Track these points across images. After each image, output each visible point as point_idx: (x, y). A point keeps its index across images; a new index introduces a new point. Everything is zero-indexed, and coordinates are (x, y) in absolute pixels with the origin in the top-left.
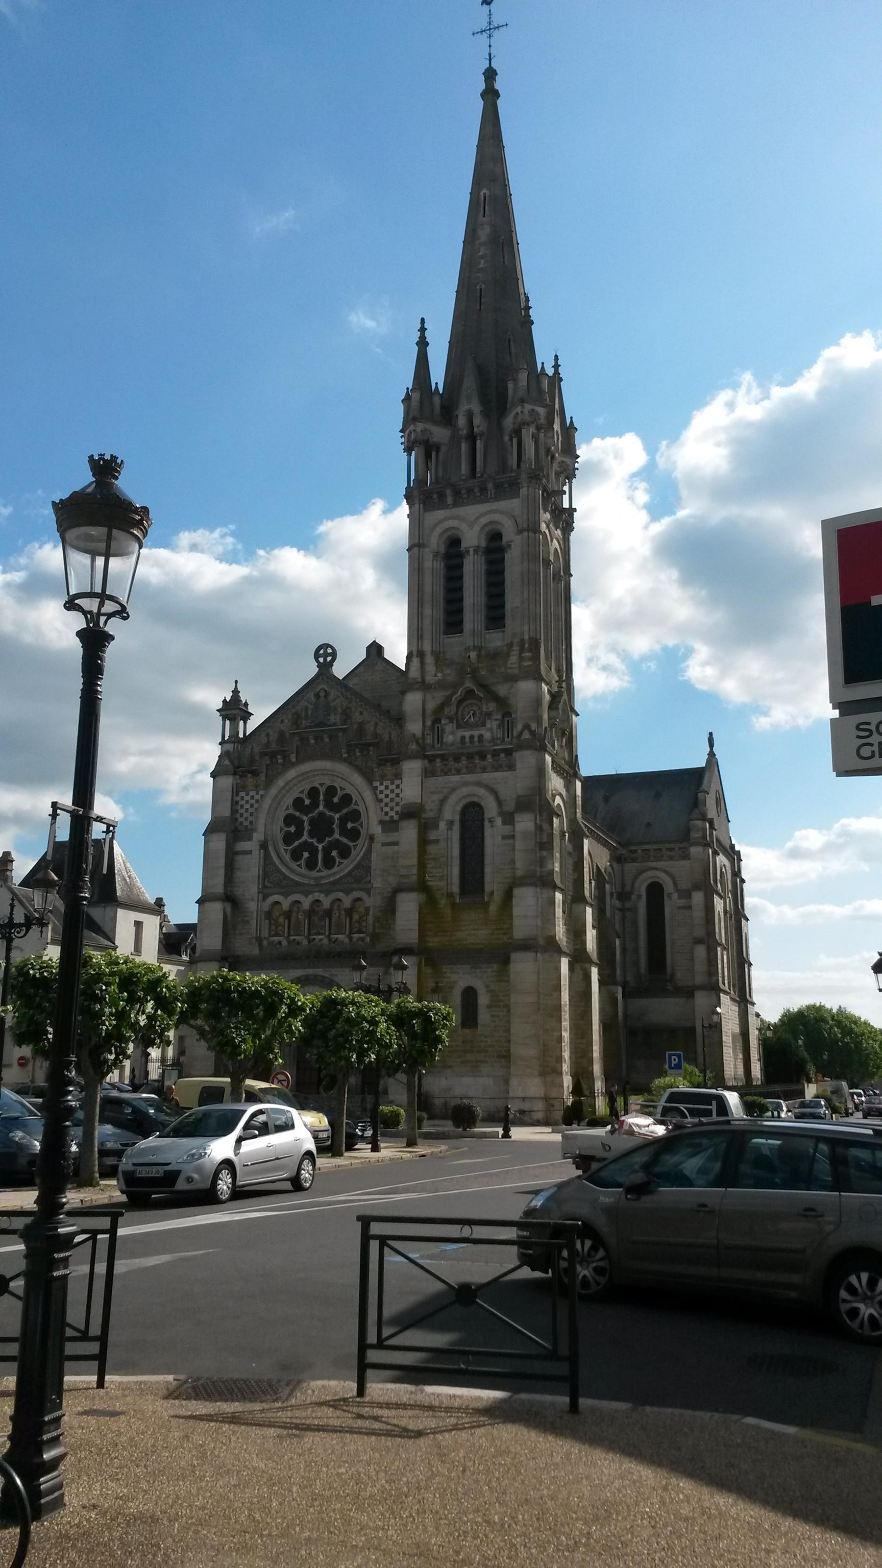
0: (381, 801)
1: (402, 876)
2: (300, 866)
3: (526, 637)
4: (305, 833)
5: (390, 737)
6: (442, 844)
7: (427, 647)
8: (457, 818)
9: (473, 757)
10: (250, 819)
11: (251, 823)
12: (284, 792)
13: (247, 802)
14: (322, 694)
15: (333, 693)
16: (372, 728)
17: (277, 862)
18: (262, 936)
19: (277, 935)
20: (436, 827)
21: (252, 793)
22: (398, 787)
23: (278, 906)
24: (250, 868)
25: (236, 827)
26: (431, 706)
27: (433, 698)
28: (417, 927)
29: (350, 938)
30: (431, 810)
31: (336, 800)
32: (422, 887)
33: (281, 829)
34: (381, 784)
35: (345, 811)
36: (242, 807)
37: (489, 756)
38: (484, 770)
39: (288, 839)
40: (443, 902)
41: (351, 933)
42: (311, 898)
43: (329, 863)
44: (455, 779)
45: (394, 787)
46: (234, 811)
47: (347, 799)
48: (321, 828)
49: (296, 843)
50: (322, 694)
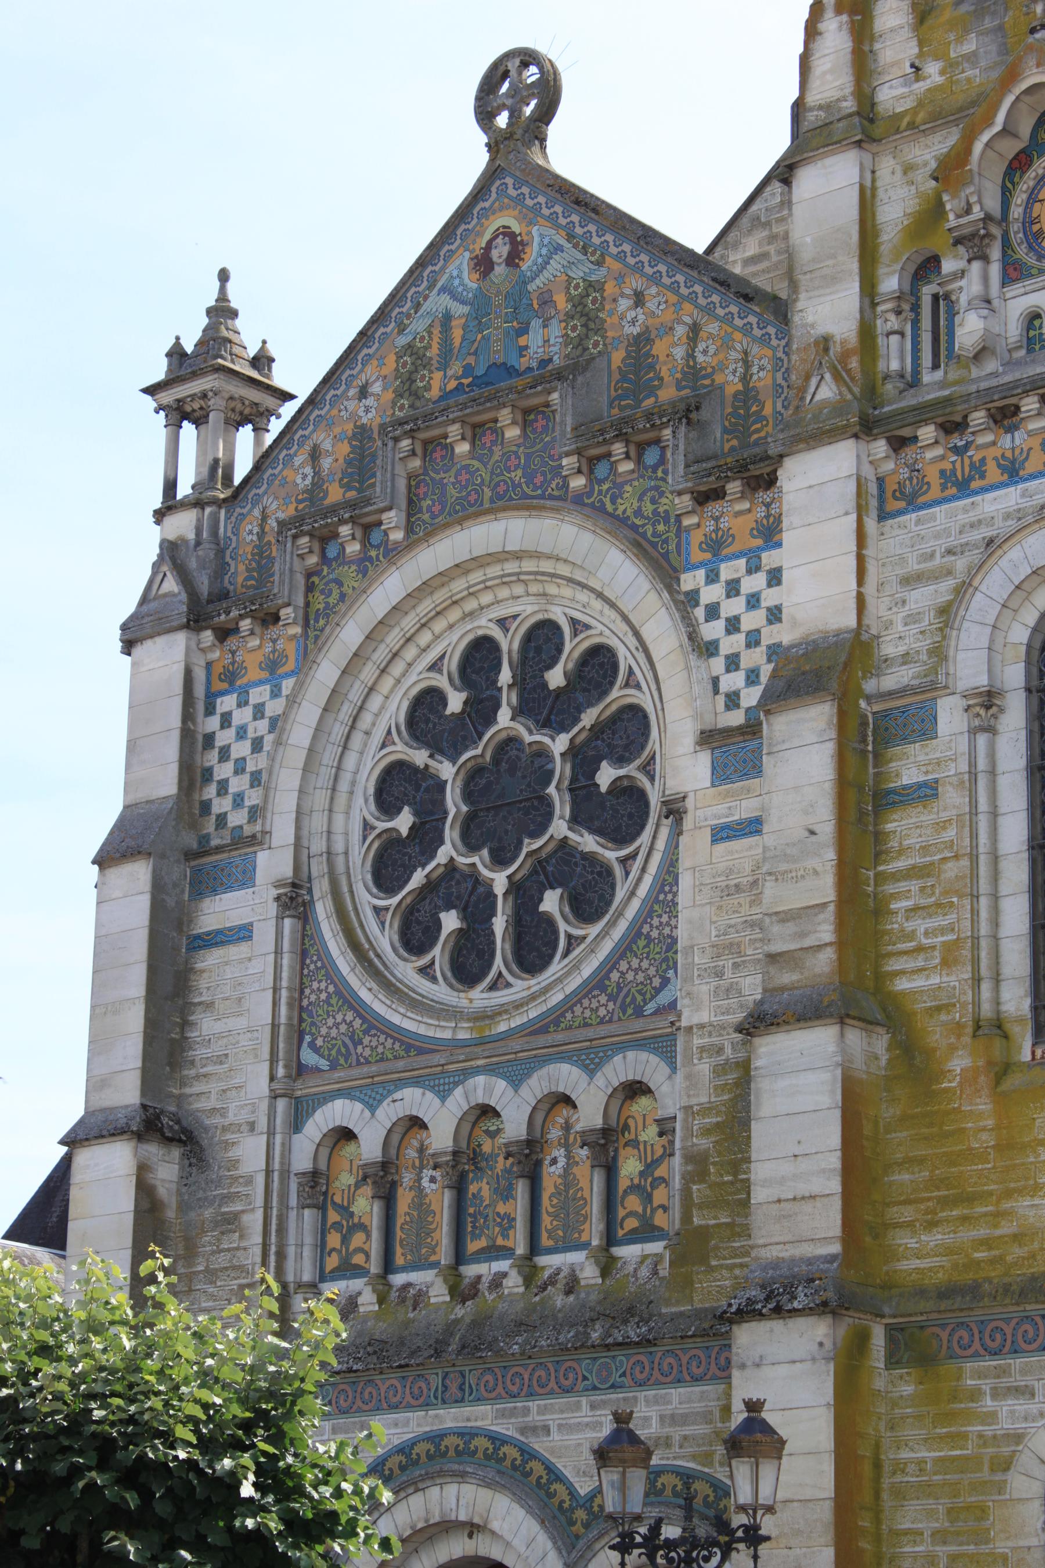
0: (710, 649)
1: (772, 958)
2: (426, 971)
5: (745, 379)
6: (953, 799)
8: (1014, 676)
10: (253, 798)
11: (254, 813)
12: (368, 673)
16: (679, 353)
17: (344, 962)
20: (927, 730)
22: (775, 578)
24: (242, 995)
25: (205, 839)
26: (896, 209)
27: (908, 169)
28: (835, 1185)
29: (607, 1266)
30: (906, 659)
31: (555, 678)
32: (857, 994)
33: (367, 827)
34: (712, 578)
35: (589, 718)
39: (389, 864)
40: (959, 1063)
41: (610, 1239)
43: (534, 947)
44: (1000, 503)
46: (192, 775)
47: (598, 667)
48: (505, 800)
49: (418, 878)
50: (500, 251)
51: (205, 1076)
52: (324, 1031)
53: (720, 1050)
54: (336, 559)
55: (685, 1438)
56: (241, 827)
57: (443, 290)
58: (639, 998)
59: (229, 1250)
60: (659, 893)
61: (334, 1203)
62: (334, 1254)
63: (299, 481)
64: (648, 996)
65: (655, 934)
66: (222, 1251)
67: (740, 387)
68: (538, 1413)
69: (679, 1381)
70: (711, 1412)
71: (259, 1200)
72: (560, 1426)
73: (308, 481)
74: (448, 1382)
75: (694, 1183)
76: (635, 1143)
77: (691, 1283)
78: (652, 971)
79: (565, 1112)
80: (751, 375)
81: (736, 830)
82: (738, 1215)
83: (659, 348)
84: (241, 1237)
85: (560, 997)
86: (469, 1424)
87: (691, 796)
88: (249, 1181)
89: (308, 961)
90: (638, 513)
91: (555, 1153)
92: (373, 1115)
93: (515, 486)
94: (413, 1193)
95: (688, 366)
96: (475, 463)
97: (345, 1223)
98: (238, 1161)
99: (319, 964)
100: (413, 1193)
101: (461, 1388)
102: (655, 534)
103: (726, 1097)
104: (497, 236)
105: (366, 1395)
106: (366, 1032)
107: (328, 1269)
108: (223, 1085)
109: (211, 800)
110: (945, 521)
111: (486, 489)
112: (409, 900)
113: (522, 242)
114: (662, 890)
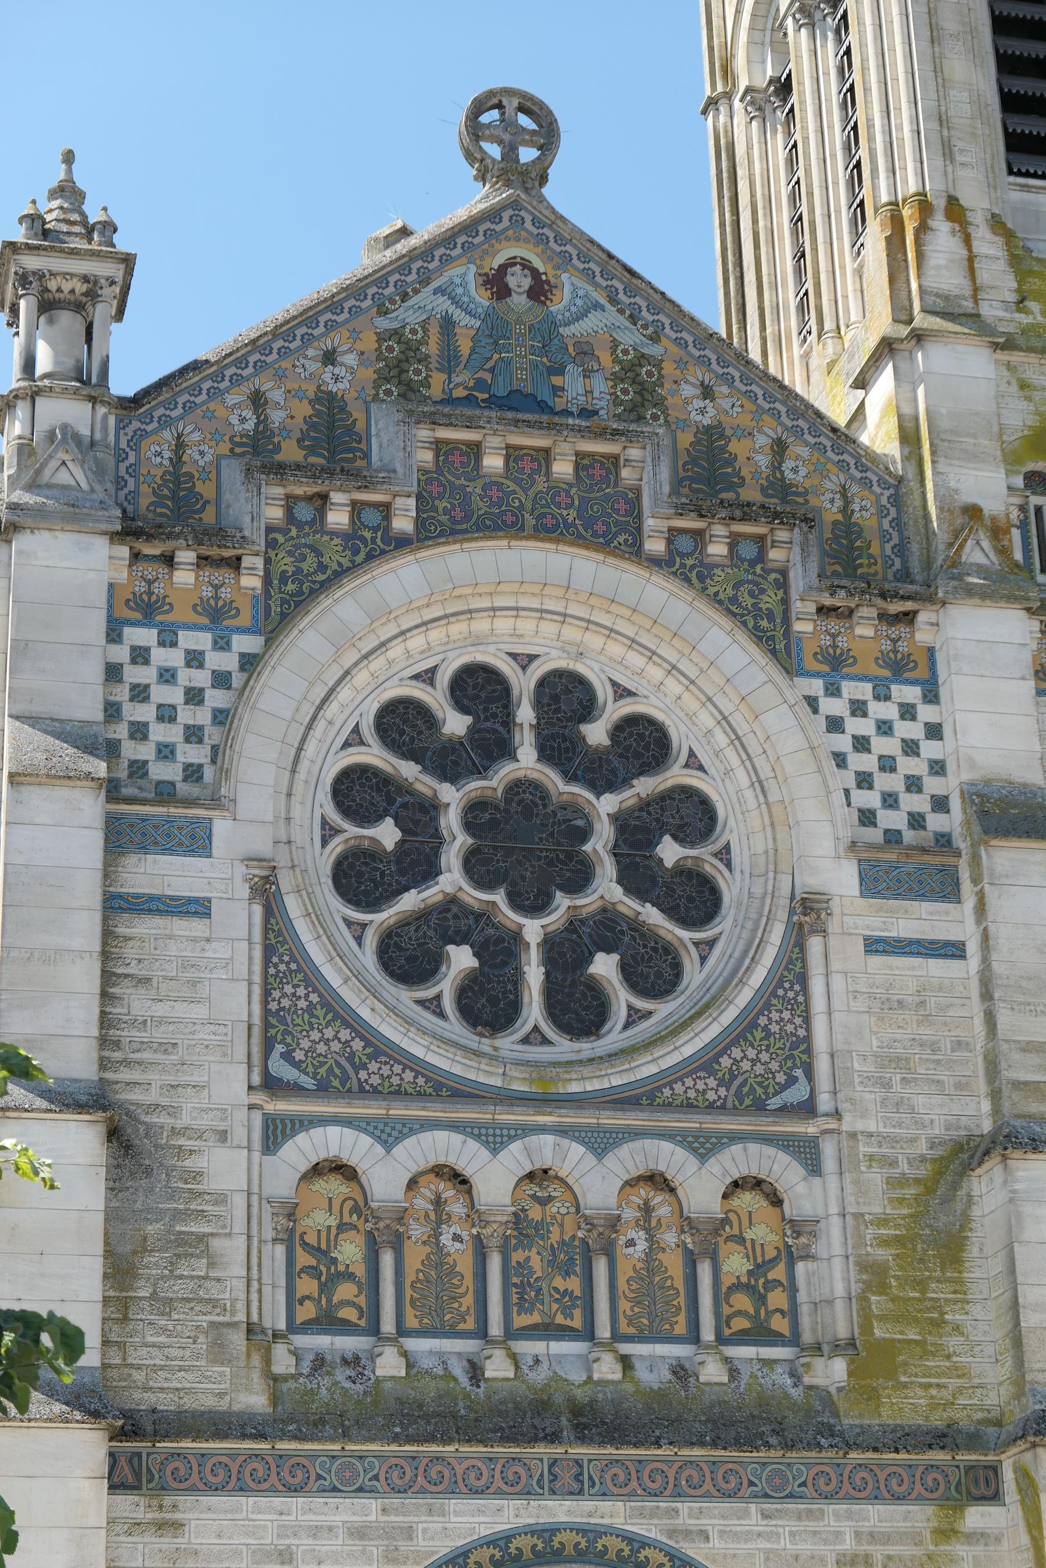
4: (452, 858)
5: (846, 510)
7: (976, 200)
10: (196, 754)
13: (167, 676)
14: (518, 281)
15: (569, 290)
16: (763, 461)
18: (267, 1323)
19: (328, 1322)
21: (188, 640)
23: (334, 1186)
31: (596, 733)
36: (140, 693)
42: (516, 1159)
45: (889, 711)
49: (410, 901)
51: (140, 1063)
52: (305, 1044)
53: (893, 1164)
54: (312, 523)
55: (889, 1558)
56: (173, 784)
57: (439, 291)
58: (759, 1091)
59: (192, 1277)
60: (776, 987)
61: (305, 1245)
62: (307, 1303)
63: (234, 420)
64: (771, 1090)
65: (774, 1028)
66: (181, 1277)
67: (839, 517)
68: (690, 1516)
69: (876, 1498)
70: (920, 1534)
71: (240, 1227)
72: (720, 1531)
73: (250, 425)
74: (556, 1470)
75: (874, 1293)
76: (740, 1240)
77: (879, 1397)
78: (774, 1066)
79: (642, 1192)
80: (853, 511)
81: (895, 947)
82: (930, 1333)
83: (734, 447)
84: (211, 1265)
85: (653, 1069)
86: (593, 1521)
87: (837, 898)
88: (221, 1199)
89: (275, 960)
90: (734, 600)
91: (631, 1234)
92: (388, 1152)
93: (568, 526)
94: (428, 1249)
95: (774, 477)
96: (513, 486)
97: (324, 1270)
98: (200, 1174)
99: (293, 966)
100: (428, 1249)
101: (578, 1477)
102: (756, 627)
103: (905, 1211)
104: (515, 264)
105: (433, 1475)
106: (371, 1057)
107: (299, 1320)
108: (171, 1079)
109: (119, 741)
111: (527, 516)
112: (392, 921)
113: (548, 282)
114: (780, 984)
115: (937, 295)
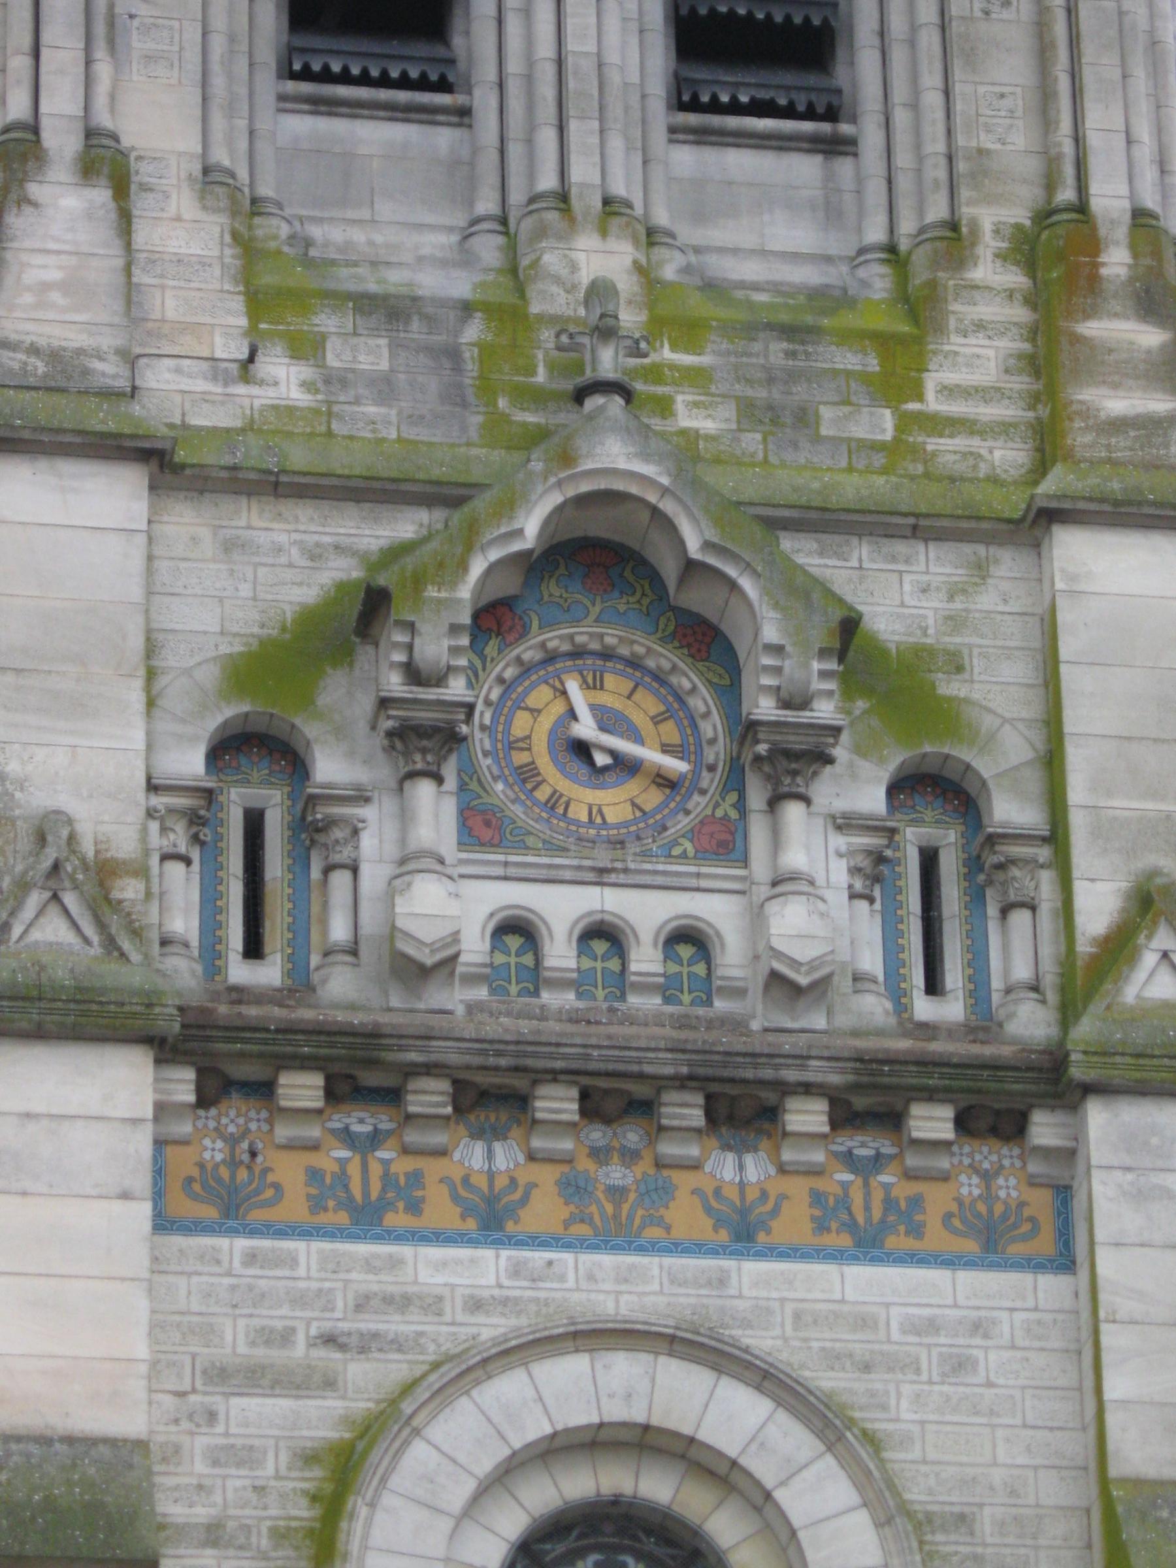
3: (1109, 198)
9: (671, 1094)
37: (807, 1116)
38: (744, 1231)
110: (318, 1272)
115: (34, 350)
